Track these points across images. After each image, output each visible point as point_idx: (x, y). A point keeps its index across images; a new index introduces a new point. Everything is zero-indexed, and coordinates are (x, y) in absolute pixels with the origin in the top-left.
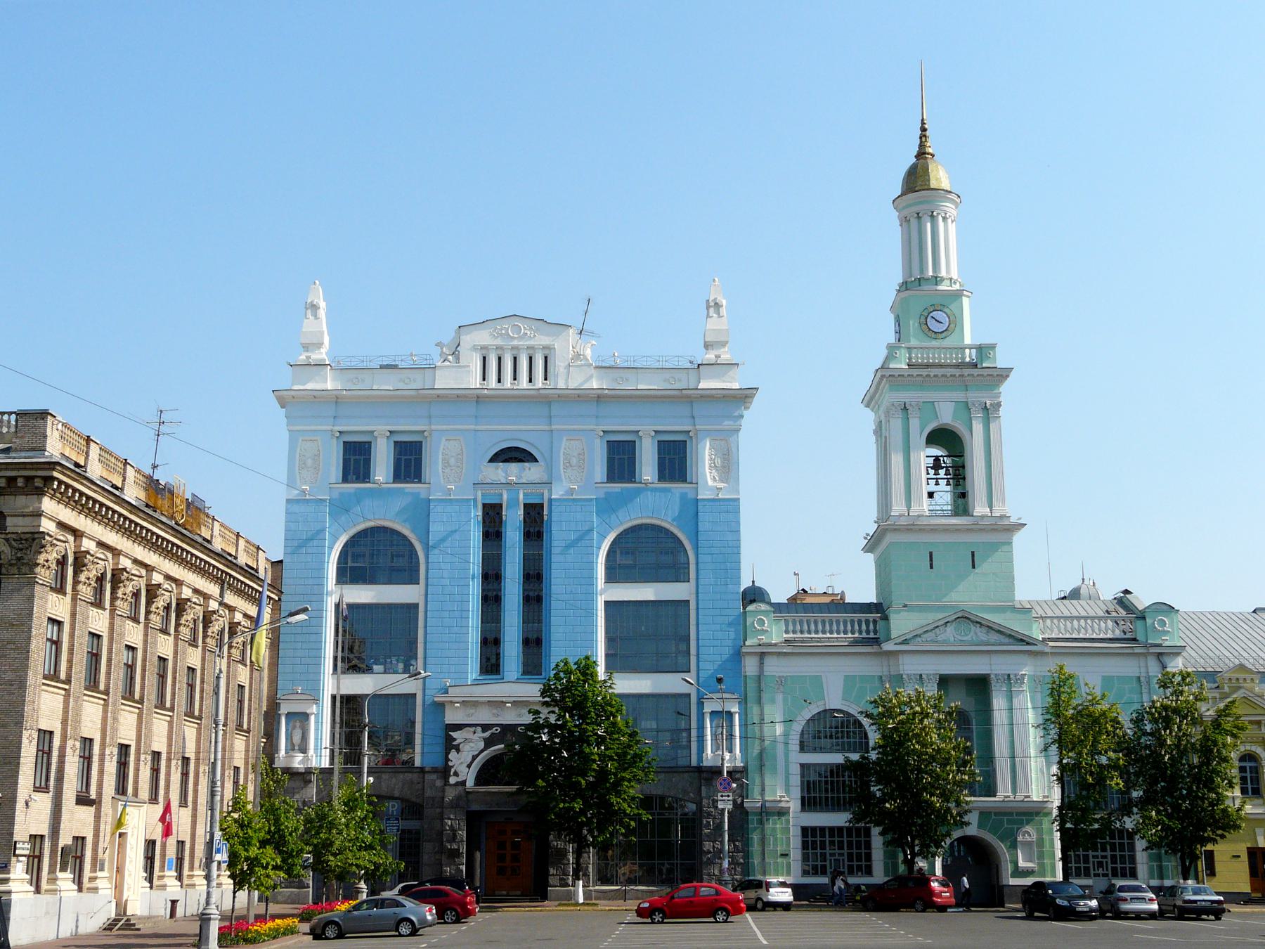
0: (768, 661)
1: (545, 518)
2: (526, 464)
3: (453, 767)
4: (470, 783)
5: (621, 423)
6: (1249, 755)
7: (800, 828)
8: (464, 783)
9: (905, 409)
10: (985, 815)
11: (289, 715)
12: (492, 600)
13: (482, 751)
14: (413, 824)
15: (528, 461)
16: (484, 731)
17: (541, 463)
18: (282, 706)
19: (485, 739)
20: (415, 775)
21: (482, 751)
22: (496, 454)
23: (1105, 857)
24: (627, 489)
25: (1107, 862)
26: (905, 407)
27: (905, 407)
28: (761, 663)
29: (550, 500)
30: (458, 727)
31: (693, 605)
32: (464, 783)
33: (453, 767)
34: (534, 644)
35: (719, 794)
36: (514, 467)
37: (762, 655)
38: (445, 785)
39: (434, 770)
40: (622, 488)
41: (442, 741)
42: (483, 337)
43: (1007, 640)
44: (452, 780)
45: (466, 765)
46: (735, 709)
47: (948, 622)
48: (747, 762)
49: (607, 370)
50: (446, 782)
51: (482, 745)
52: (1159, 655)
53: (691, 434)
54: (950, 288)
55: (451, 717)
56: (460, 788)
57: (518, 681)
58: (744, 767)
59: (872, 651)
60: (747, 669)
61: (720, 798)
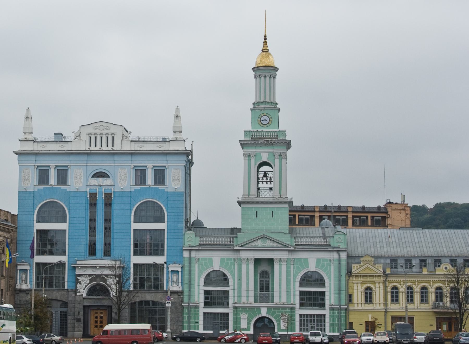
1: (112, 198)
2: (105, 178)
3: (78, 289)
4: (85, 295)
5: (140, 162)
6: (369, 288)
7: (203, 313)
8: (82, 295)
9: (249, 156)
10: (269, 308)
11: (20, 270)
12: (93, 229)
13: (89, 284)
14: (64, 310)
15: (106, 177)
16: (89, 277)
17: (111, 178)
18: (18, 266)
19: (89, 279)
20: (65, 292)
21: (89, 284)
22: (95, 174)
23: (314, 324)
24: (142, 188)
25: (315, 326)
28: (190, 254)
29: (114, 192)
30: (80, 275)
31: (166, 231)
32: (82, 295)
33: (78, 289)
34: (107, 245)
35: (167, 302)
36: (100, 180)
37: (190, 250)
38: (76, 296)
39: (72, 291)
40: (141, 188)
41: (74, 281)
42: (90, 130)
43: (280, 246)
44: (78, 294)
45: (83, 289)
46: (179, 269)
47: (259, 239)
48: (184, 290)
49: (135, 143)
50: (76, 295)
51: (88, 282)
53: (166, 167)
55: (78, 272)
56: (81, 297)
57: (102, 259)
58: (182, 291)
59: (231, 249)
60: (185, 255)
61: (167, 303)
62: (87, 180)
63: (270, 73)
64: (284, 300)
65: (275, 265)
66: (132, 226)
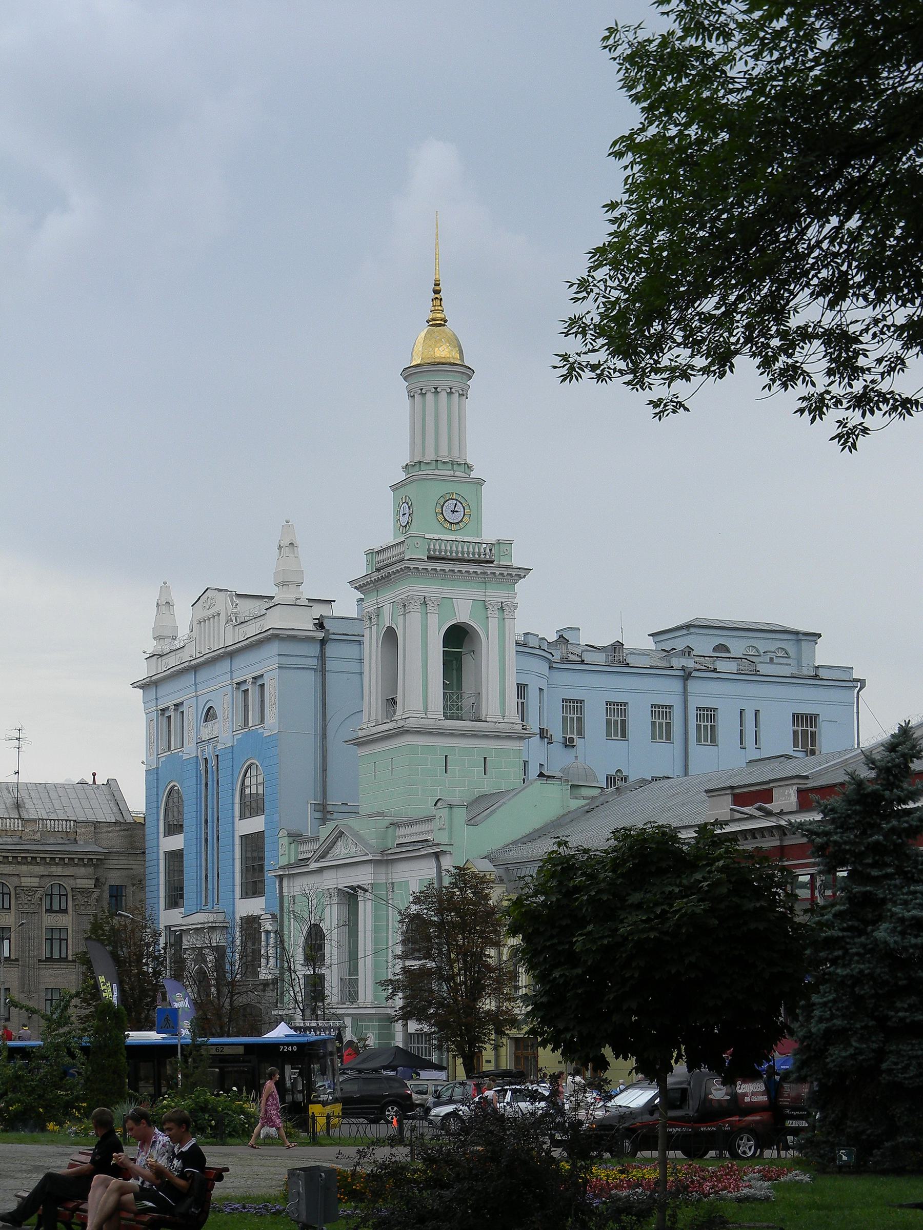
0: (285, 883)
10: (356, 1018)
26: (425, 602)
27: (425, 602)
37: (281, 878)
52: (437, 855)
54: (420, 473)
62: (198, 731)
63: (419, 384)
64: (370, 998)
65: (361, 904)
66: (236, 828)
